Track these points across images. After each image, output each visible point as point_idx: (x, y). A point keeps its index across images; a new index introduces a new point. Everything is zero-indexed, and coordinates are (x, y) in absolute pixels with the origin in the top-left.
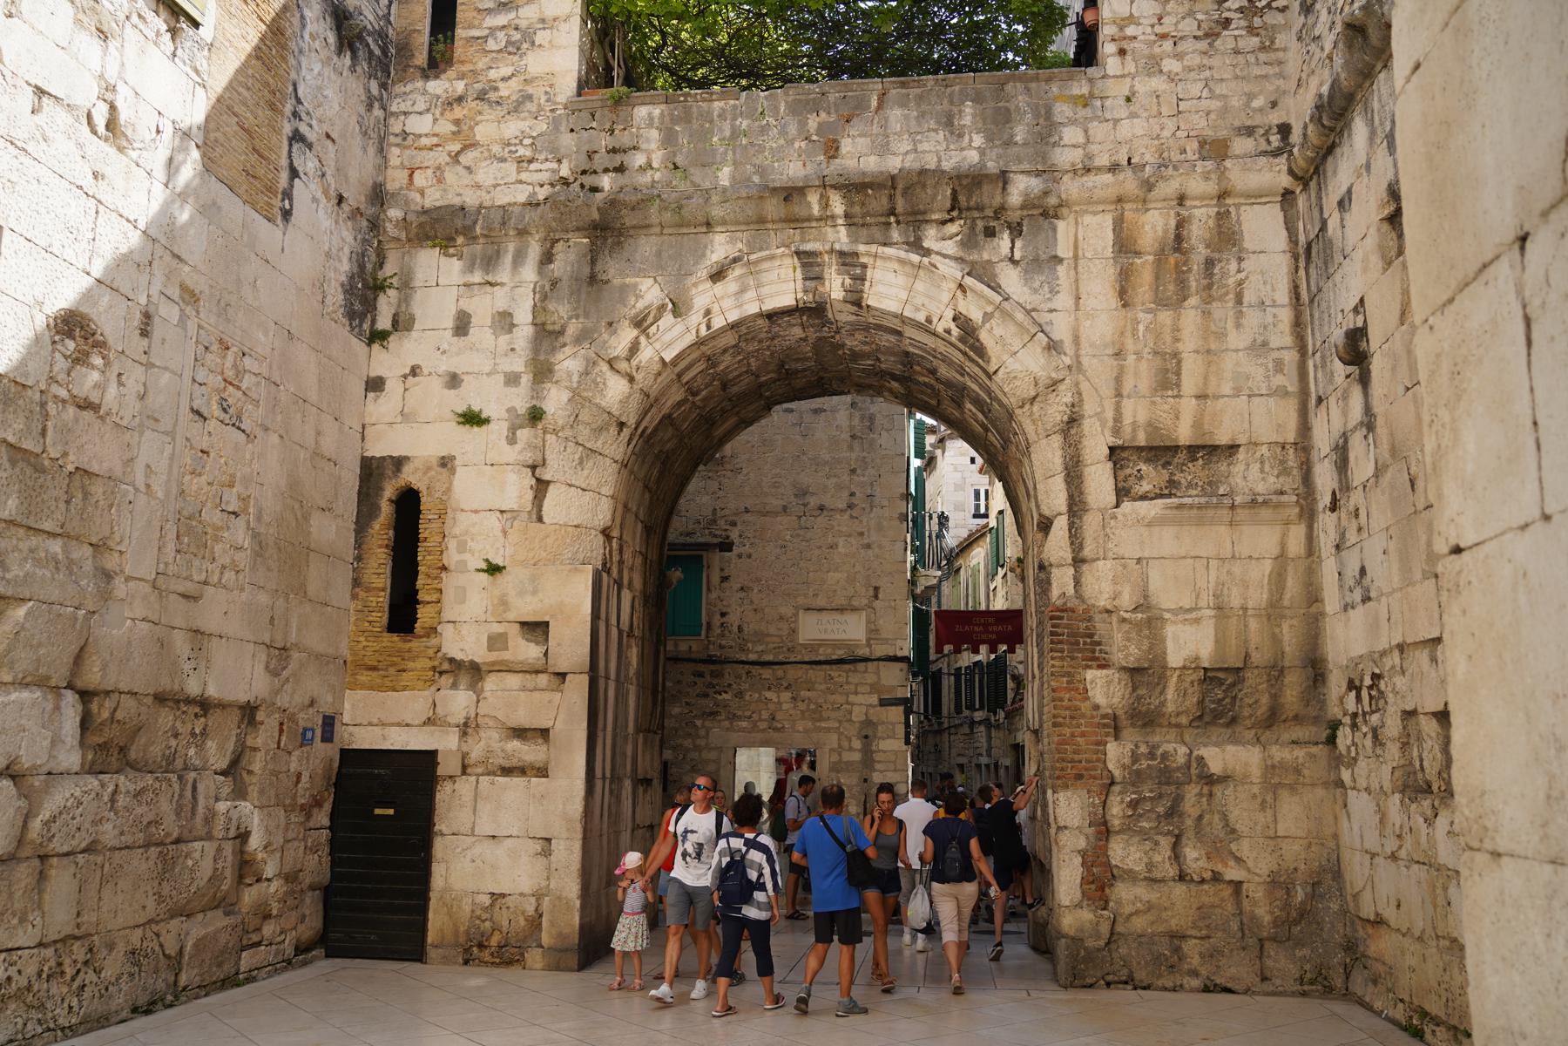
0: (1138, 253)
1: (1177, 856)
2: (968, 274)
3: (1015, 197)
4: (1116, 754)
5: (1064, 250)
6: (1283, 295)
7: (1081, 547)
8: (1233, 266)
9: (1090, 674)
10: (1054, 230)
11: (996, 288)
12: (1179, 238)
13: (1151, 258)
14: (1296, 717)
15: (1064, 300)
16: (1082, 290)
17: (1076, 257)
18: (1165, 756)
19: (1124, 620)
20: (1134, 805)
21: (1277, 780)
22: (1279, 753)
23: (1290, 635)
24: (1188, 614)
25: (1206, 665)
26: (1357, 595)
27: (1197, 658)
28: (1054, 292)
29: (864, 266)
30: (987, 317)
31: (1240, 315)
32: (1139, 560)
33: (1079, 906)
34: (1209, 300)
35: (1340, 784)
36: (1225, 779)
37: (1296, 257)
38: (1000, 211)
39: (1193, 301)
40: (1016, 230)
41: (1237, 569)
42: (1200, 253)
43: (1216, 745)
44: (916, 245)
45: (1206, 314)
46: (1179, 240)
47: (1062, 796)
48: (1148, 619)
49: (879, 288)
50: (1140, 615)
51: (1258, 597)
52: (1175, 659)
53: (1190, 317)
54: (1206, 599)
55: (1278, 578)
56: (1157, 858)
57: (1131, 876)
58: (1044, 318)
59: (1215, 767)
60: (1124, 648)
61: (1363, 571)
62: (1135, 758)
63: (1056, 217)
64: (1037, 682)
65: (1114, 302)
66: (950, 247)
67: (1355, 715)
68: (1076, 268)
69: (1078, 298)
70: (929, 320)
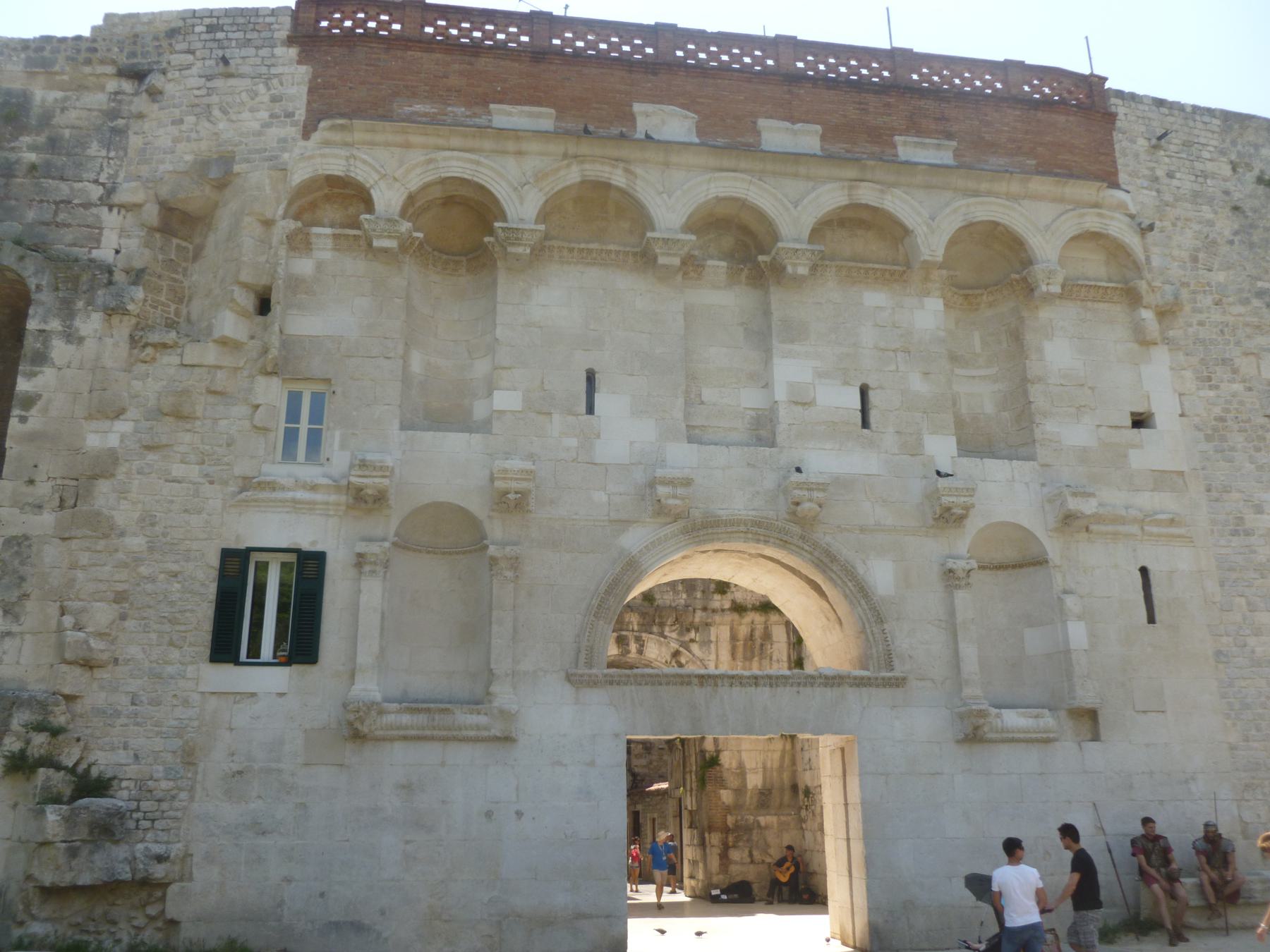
0: (738, 640)
1: (751, 855)
2: (680, 646)
3: (697, 620)
4: (730, 820)
5: (713, 638)
6: (785, 658)
7: (718, 746)
8: (769, 647)
9: (722, 792)
10: (710, 630)
11: (690, 651)
12: (752, 635)
13: (742, 642)
14: (788, 806)
15: (713, 657)
16: (720, 653)
17: (717, 642)
18: (747, 819)
19: (733, 773)
20: (736, 837)
21: (783, 827)
22: (783, 818)
23: (786, 776)
24: (754, 771)
25: (759, 787)
26: (808, 767)
27: (756, 786)
28: (710, 653)
29: (644, 641)
30: (687, 662)
31: (771, 664)
32: (738, 751)
33: (718, 874)
34: (761, 659)
35: (802, 828)
36: (767, 827)
37: (789, 645)
38: (692, 624)
39: (756, 659)
40: (697, 630)
41: (770, 754)
42: (758, 642)
43: (763, 815)
44: (662, 635)
45: (760, 664)
46: (751, 636)
47: (712, 835)
48: (741, 772)
49: (649, 649)
50: (738, 771)
51: (776, 765)
52: (750, 786)
53: (755, 664)
54: (760, 765)
55: (782, 757)
56: (744, 856)
57: (736, 863)
58: (706, 663)
59: (763, 824)
60: (733, 782)
61: (810, 760)
62: (737, 821)
63: (711, 625)
64: (694, 793)
65: (730, 658)
66: (674, 635)
67: (807, 806)
68: (717, 645)
69: (717, 656)
70: (666, 662)
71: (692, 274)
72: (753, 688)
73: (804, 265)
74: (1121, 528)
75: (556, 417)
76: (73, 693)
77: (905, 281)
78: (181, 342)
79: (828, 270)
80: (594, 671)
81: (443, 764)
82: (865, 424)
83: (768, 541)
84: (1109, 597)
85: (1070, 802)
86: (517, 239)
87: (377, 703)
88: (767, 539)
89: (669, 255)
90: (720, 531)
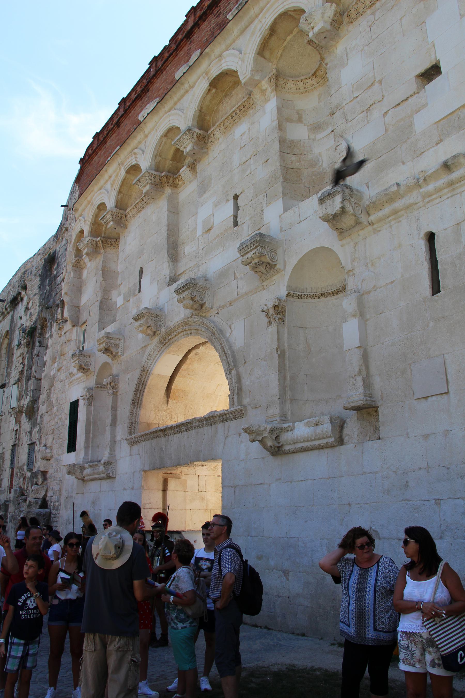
71: (180, 183)
72: (181, 434)
73: (189, 144)
74: (398, 204)
75: (131, 300)
76: (44, 470)
77: (253, 104)
78: (64, 324)
79: (216, 132)
80: (133, 436)
81: (100, 492)
82: (236, 224)
83: (191, 333)
84: (392, 283)
85: (349, 504)
86: (107, 221)
87: (77, 464)
88: (191, 331)
89: (145, 186)
90: (173, 336)
